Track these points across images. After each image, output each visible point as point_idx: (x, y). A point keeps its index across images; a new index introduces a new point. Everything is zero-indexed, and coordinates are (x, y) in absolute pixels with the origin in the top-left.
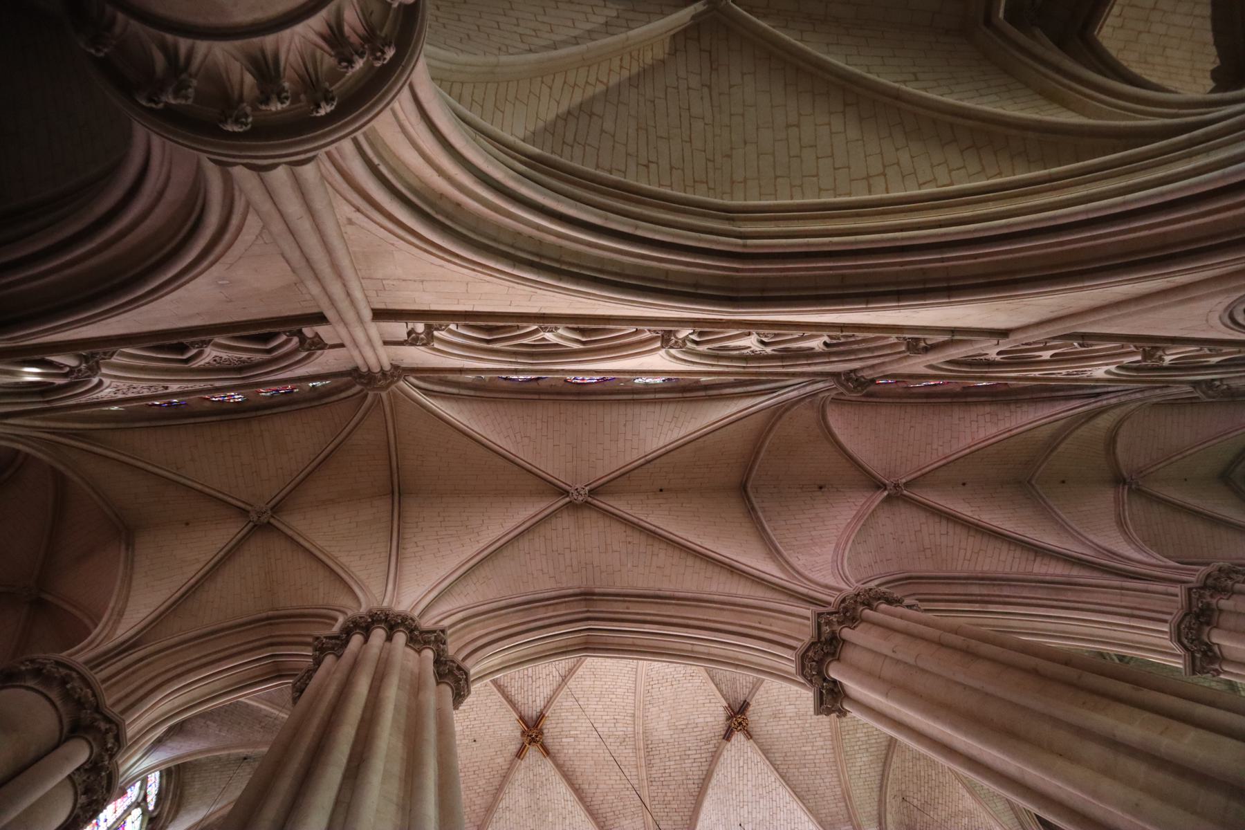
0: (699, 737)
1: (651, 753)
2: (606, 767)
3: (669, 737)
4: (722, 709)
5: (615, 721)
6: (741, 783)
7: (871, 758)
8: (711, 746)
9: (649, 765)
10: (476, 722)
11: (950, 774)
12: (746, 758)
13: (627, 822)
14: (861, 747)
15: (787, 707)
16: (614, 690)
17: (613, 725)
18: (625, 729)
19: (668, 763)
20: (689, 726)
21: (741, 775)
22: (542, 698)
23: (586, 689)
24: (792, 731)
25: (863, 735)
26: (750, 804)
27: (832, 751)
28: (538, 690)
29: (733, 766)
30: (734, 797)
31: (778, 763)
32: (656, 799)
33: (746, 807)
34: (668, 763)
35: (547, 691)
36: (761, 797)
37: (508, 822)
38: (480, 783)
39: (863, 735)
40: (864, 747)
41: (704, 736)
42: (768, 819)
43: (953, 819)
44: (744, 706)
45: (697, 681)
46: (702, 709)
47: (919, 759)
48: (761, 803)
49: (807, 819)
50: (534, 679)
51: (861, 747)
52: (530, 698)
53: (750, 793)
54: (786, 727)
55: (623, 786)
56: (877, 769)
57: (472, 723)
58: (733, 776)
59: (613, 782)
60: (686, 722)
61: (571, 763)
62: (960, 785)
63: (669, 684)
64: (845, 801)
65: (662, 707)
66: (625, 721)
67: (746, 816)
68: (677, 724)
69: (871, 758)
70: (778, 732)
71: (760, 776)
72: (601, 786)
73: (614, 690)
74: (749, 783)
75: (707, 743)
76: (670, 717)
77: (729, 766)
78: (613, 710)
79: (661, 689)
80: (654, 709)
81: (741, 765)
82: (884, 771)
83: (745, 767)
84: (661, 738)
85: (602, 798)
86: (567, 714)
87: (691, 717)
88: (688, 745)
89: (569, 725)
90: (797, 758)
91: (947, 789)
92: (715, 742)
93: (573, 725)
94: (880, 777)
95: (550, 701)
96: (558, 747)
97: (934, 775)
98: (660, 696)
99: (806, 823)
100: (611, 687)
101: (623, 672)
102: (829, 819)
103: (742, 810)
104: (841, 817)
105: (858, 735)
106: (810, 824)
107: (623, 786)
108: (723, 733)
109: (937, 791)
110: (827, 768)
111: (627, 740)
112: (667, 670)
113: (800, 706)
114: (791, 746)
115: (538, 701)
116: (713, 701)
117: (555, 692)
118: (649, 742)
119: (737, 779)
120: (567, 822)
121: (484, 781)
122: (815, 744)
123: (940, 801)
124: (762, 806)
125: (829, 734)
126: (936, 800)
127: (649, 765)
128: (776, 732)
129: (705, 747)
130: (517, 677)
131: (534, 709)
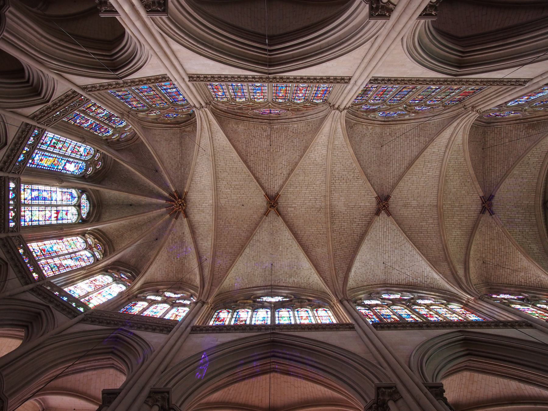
0: (361, 213)
1: (334, 217)
2: (310, 223)
3: (344, 210)
4: (375, 199)
5: (315, 199)
6: (385, 240)
7: (462, 233)
8: (368, 218)
9: (332, 223)
10: (244, 195)
11: (513, 246)
12: (388, 227)
13: (319, 249)
14: (456, 226)
15: (412, 201)
16: (315, 182)
17: (314, 202)
18: (320, 204)
19: (343, 224)
20: (356, 207)
21: (385, 236)
22: (278, 186)
23: (301, 182)
24: (415, 214)
25: (458, 220)
26: (389, 252)
27: (438, 225)
28: (276, 181)
29: (380, 231)
30: (381, 248)
31: (406, 230)
32: (336, 239)
33: (387, 254)
34: (343, 224)
35: (280, 182)
36: (396, 249)
37: (258, 248)
38: (245, 226)
39: (458, 220)
40: (458, 226)
41: (364, 213)
42: (399, 260)
43: (514, 273)
44: (388, 198)
45: (361, 182)
46: (364, 198)
47: (494, 239)
48: (396, 252)
49: (421, 259)
50: (274, 176)
51: (456, 226)
52: (272, 185)
53: (390, 247)
54: (411, 212)
55: (318, 233)
56: (466, 239)
57: (242, 196)
58: (380, 236)
59: (313, 230)
60: (354, 204)
61: (292, 220)
62: (519, 253)
63: (345, 181)
64: (444, 251)
65: (341, 194)
66: (320, 200)
67: (387, 258)
68: (349, 204)
69: (462, 233)
70: (407, 214)
71: (395, 237)
72: (307, 232)
73: (315, 182)
74: (390, 241)
75: (366, 216)
76: (345, 200)
77: (378, 230)
79: (340, 183)
80: (337, 194)
81: (385, 231)
82: (470, 240)
83: (387, 232)
84: (340, 210)
85: (306, 238)
86: (291, 195)
87: (357, 202)
88: (355, 216)
90: (417, 228)
91: (511, 256)
92: (371, 216)
93: (294, 201)
94: (467, 243)
95: (281, 187)
96: (286, 213)
97: (503, 248)
98: (340, 188)
99: (421, 261)
101: (319, 171)
102: (435, 259)
103: (385, 255)
104: (441, 258)
105: (454, 220)
106: (423, 261)
107: (318, 233)
108: (375, 212)
109: (505, 257)
110: (434, 234)
111: (321, 209)
112: (343, 173)
113: (420, 201)
114: (414, 222)
116: (369, 194)
117: (284, 182)
118: (333, 212)
119: (383, 238)
120: (289, 250)
121: (247, 226)
122: (428, 221)
123: (507, 264)
124: (396, 254)
125: (437, 216)
126: (504, 263)
127: (332, 223)
128: (405, 214)
129: (365, 218)
130: (265, 174)
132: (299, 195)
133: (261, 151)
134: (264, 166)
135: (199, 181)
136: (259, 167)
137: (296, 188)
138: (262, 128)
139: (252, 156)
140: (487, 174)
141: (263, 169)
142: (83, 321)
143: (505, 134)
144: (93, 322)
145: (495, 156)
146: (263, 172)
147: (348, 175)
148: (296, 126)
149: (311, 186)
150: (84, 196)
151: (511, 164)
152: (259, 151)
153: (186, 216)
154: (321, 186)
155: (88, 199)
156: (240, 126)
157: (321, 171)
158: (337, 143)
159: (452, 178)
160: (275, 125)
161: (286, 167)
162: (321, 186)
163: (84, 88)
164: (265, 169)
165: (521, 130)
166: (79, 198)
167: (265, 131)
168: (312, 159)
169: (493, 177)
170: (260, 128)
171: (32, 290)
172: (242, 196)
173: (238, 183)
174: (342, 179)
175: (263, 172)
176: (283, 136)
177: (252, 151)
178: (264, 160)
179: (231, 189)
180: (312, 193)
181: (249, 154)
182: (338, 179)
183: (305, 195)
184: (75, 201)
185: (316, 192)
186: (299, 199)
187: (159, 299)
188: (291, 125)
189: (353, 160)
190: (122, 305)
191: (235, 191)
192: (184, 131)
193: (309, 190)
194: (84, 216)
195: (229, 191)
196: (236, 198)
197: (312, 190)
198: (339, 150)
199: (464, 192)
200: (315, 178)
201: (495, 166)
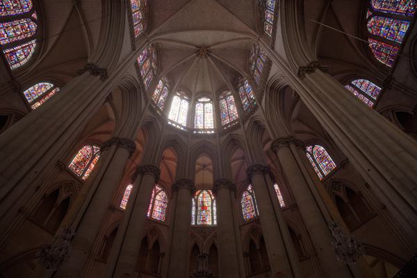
142: (260, 104)
144: (262, 98)
150: (200, 100)
153: (209, 47)
155: (200, 98)
163: (147, 103)
166: (199, 102)
171: (243, 124)
184: (202, 105)
187: (254, 63)
190: (255, 83)
194: (209, 100)
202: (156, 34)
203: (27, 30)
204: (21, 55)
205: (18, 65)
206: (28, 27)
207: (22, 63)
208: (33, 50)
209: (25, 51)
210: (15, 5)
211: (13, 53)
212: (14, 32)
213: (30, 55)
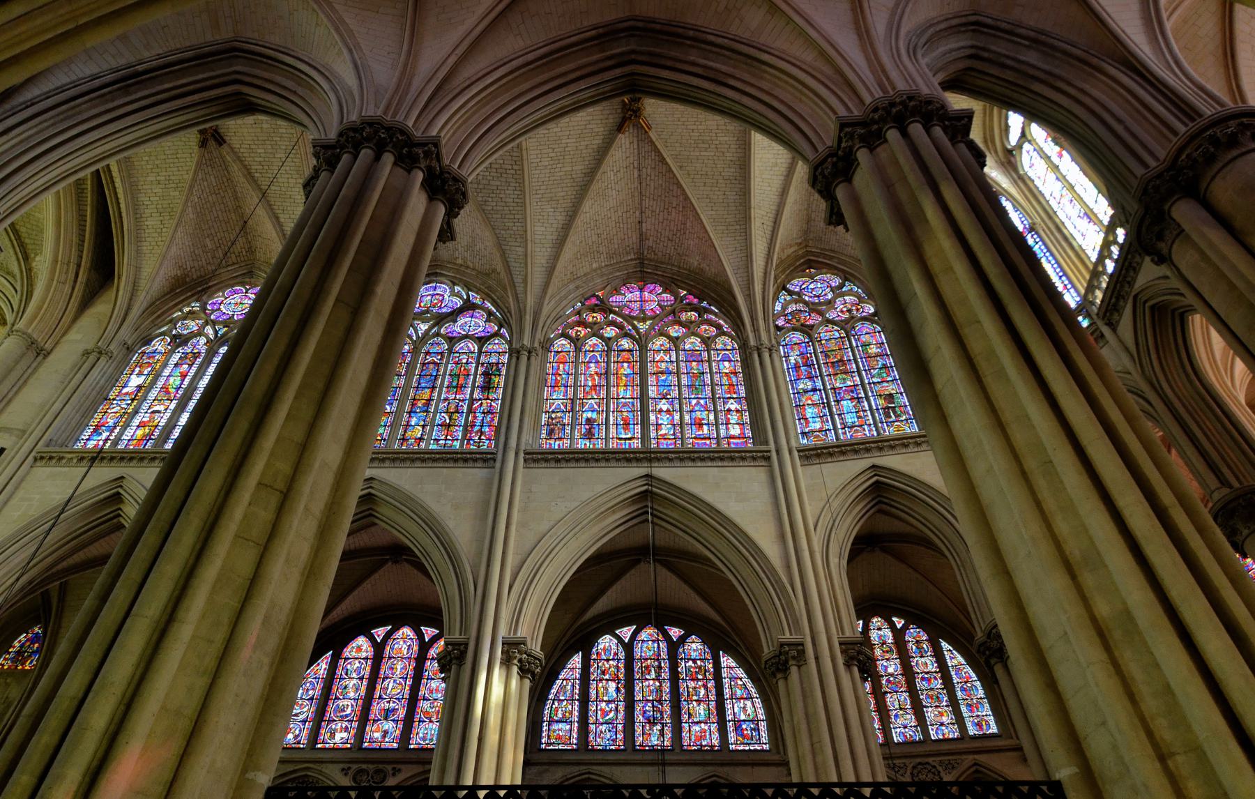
10: (692, 127)
16: (552, 162)
23: (579, 160)
28: (628, 155)
57: (695, 127)
73: (552, 162)
78: (551, 139)
79: (502, 162)
86: (597, 130)
89: (595, 117)
100: (554, 166)
101: (544, 187)
112: (499, 183)
115: (627, 143)
131: (631, 135)
132: (580, 132)
133: (657, 212)
134: (652, 184)
135: (780, 156)
136: (660, 182)
137: (587, 145)
138: (655, 254)
139: (674, 206)
140: (225, 180)
141: (652, 178)
143: (217, 255)
145: (220, 213)
146: (653, 174)
147: (489, 178)
148: (595, 265)
149: (559, 154)
151: (190, 208)
152: (661, 213)
154: (539, 156)
156: (696, 263)
157: (542, 187)
158: (517, 249)
159: (290, 180)
160: (631, 260)
161: (610, 186)
162: (539, 156)
164: (648, 178)
165: (193, 270)
167: (650, 248)
168: (561, 210)
169: (212, 177)
170: (660, 254)
172: (695, 127)
173: (702, 153)
174: (499, 171)
175: (653, 174)
176: (615, 241)
177: (673, 214)
178: (652, 196)
179: (718, 142)
180: (555, 138)
181: (681, 209)
182: (508, 171)
183: (568, 133)
185: (548, 143)
186: (580, 123)
188: (603, 264)
189: (484, 210)
191: (709, 138)
192: (800, 244)
193: (561, 145)
195: (721, 139)
196: (708, 123)
197: (557, 146)
198: (512, 232)
199: (259, 151)
200: (552, 171)
201: (214, 196)
202: (749, 297)
203: (700, 668)
204: (744, 709)
205: (763, 726)
206: (694, 661)
207: (761, 716)
208: (740, 672)
209: (739, 692)
210: (653, 675)
211: (738, 724)
212: (699, 701)
213: (749, 685)
